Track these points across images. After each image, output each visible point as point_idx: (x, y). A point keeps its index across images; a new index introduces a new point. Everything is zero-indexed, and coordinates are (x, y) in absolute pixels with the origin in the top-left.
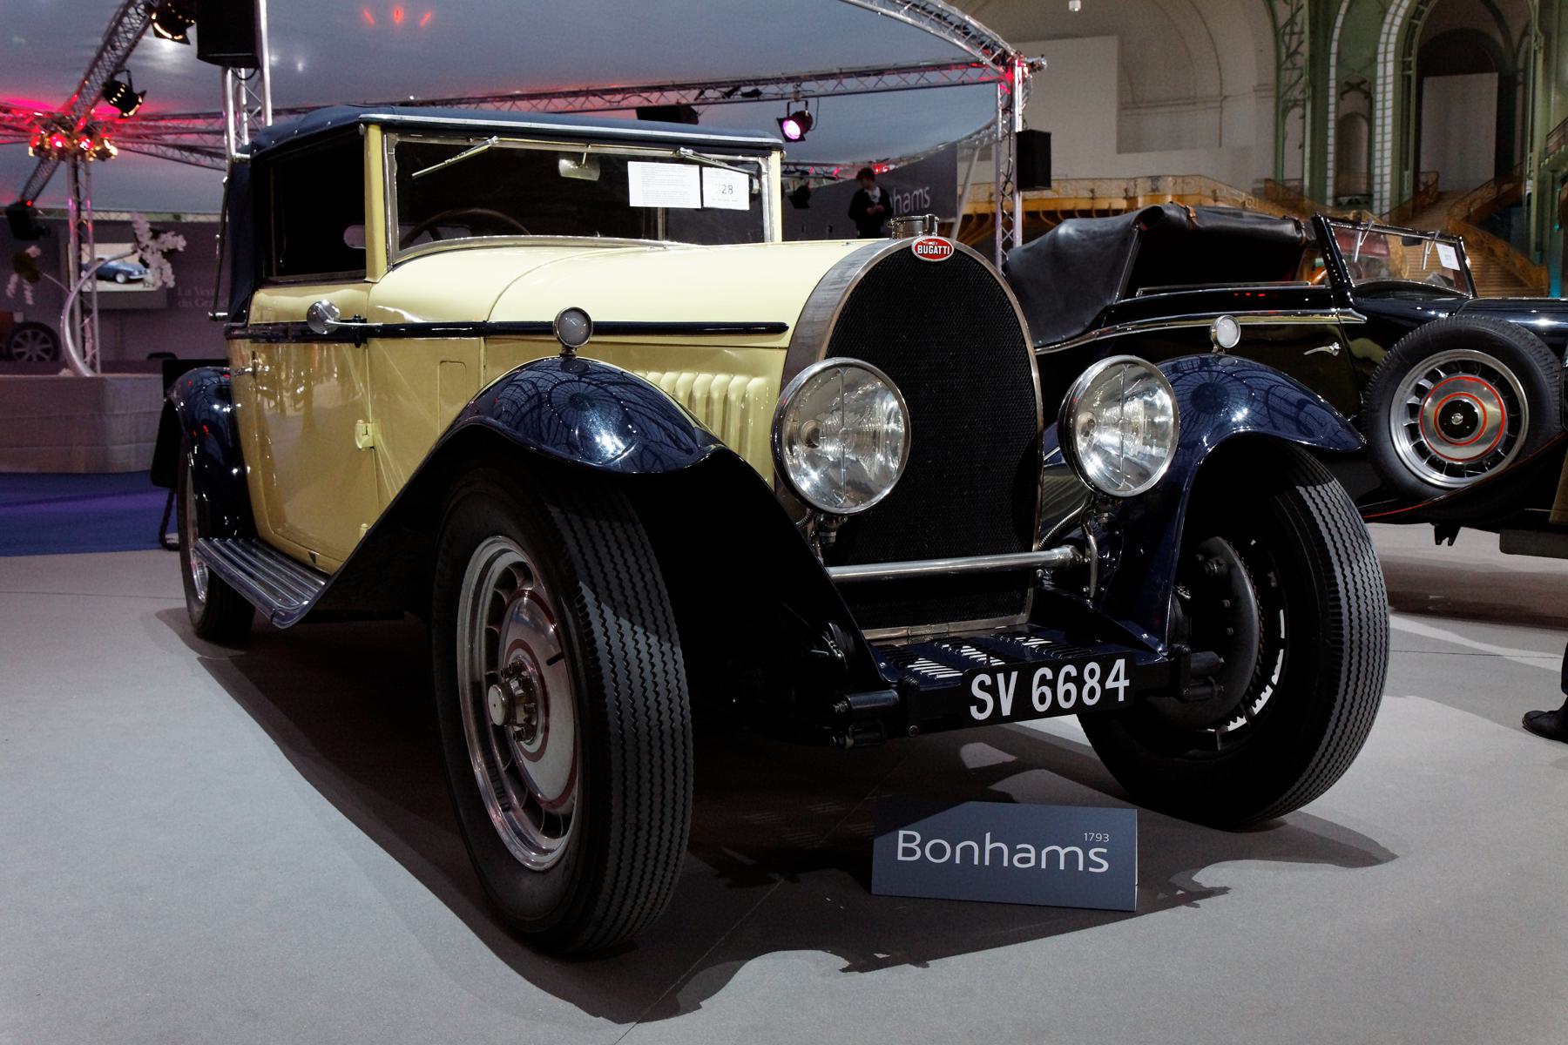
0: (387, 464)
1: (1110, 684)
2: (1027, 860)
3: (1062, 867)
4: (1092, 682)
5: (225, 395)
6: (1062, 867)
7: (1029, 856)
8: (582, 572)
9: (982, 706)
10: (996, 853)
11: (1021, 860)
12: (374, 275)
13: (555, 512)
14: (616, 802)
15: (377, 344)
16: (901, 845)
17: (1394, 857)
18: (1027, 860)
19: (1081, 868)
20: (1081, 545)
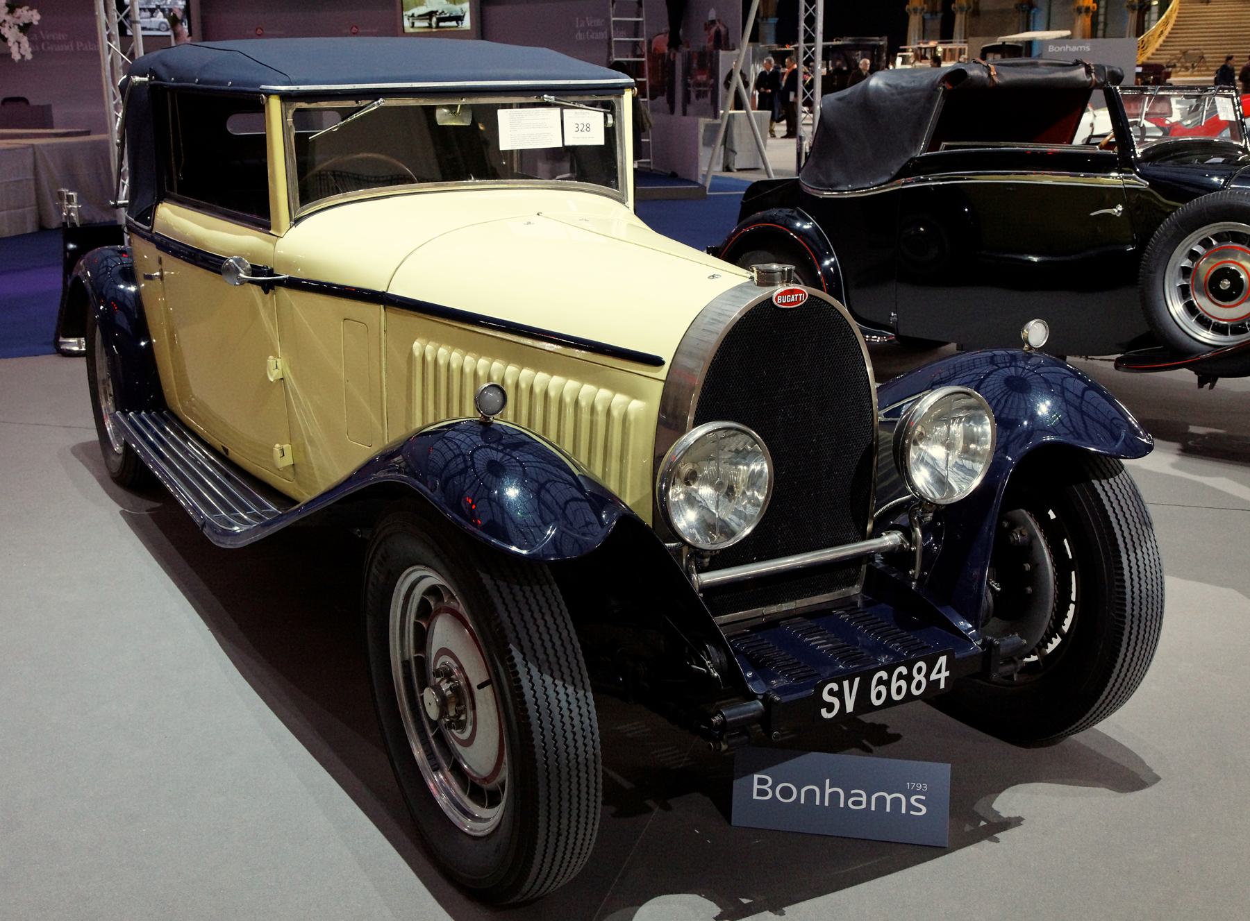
0: (295, 393)
2: (860, 803)
3: (888, 810)
5: (129, 275)
6: (888, 810)
7: (861, 800)
8: (511, 636)
10: (834, 796)
11: (855, 803)
12: (279, 230)
13: (486, 579)
15: (284, 292)
18: (860, 803)
19: (904, 811)
20: (907, 532)
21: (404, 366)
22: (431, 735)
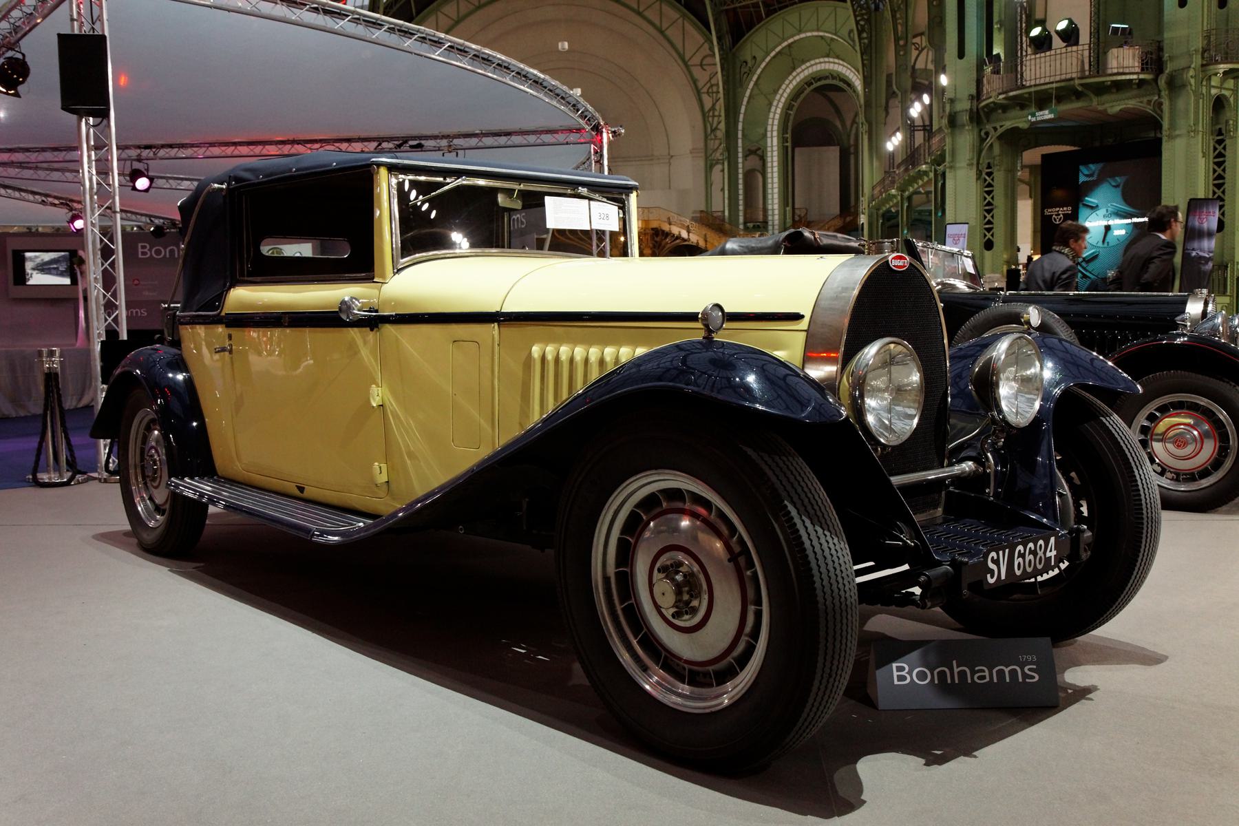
0: (396, 416)
1: (1048, 554)
2: (983, 677)
4: (1040, 553)
5: (179, 364)
8: (784, 494)
9: (992, 572)
10: (962, 674)
11: (979, 678)
12: (383, 276)
13: (750, 452)
14: (820, 659)
15: (389, 329)
16: (895, 674)
17: (1166, 658)
18: (983, 677)
21: (518, 370)
22: (634, 642)
